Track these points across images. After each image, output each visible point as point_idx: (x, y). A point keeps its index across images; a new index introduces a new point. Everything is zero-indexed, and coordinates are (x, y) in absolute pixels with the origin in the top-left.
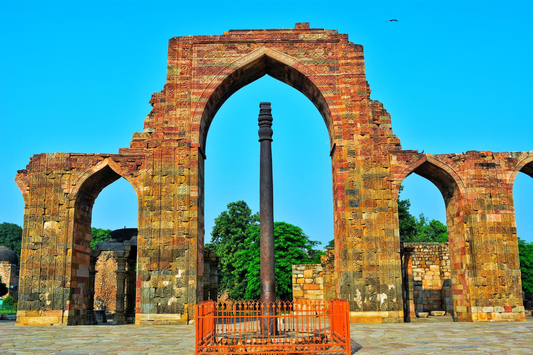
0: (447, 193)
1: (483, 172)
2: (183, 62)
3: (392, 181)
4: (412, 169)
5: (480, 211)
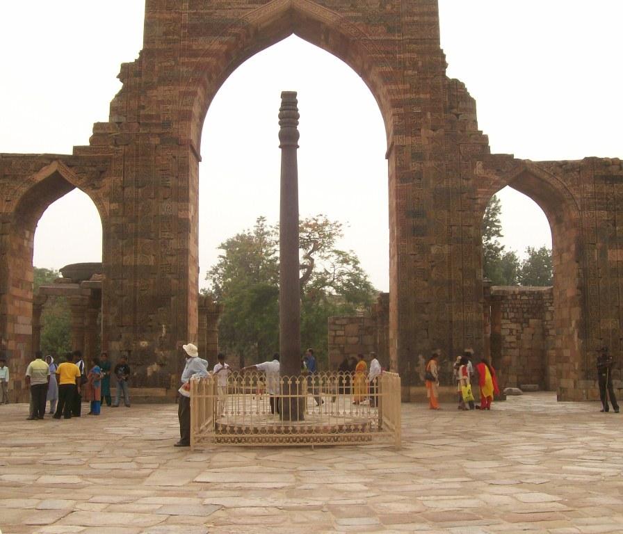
0: (554, 217)
1: (606, 189)
2: (168, 16)
3: (475, 199)
5: (599, 245)
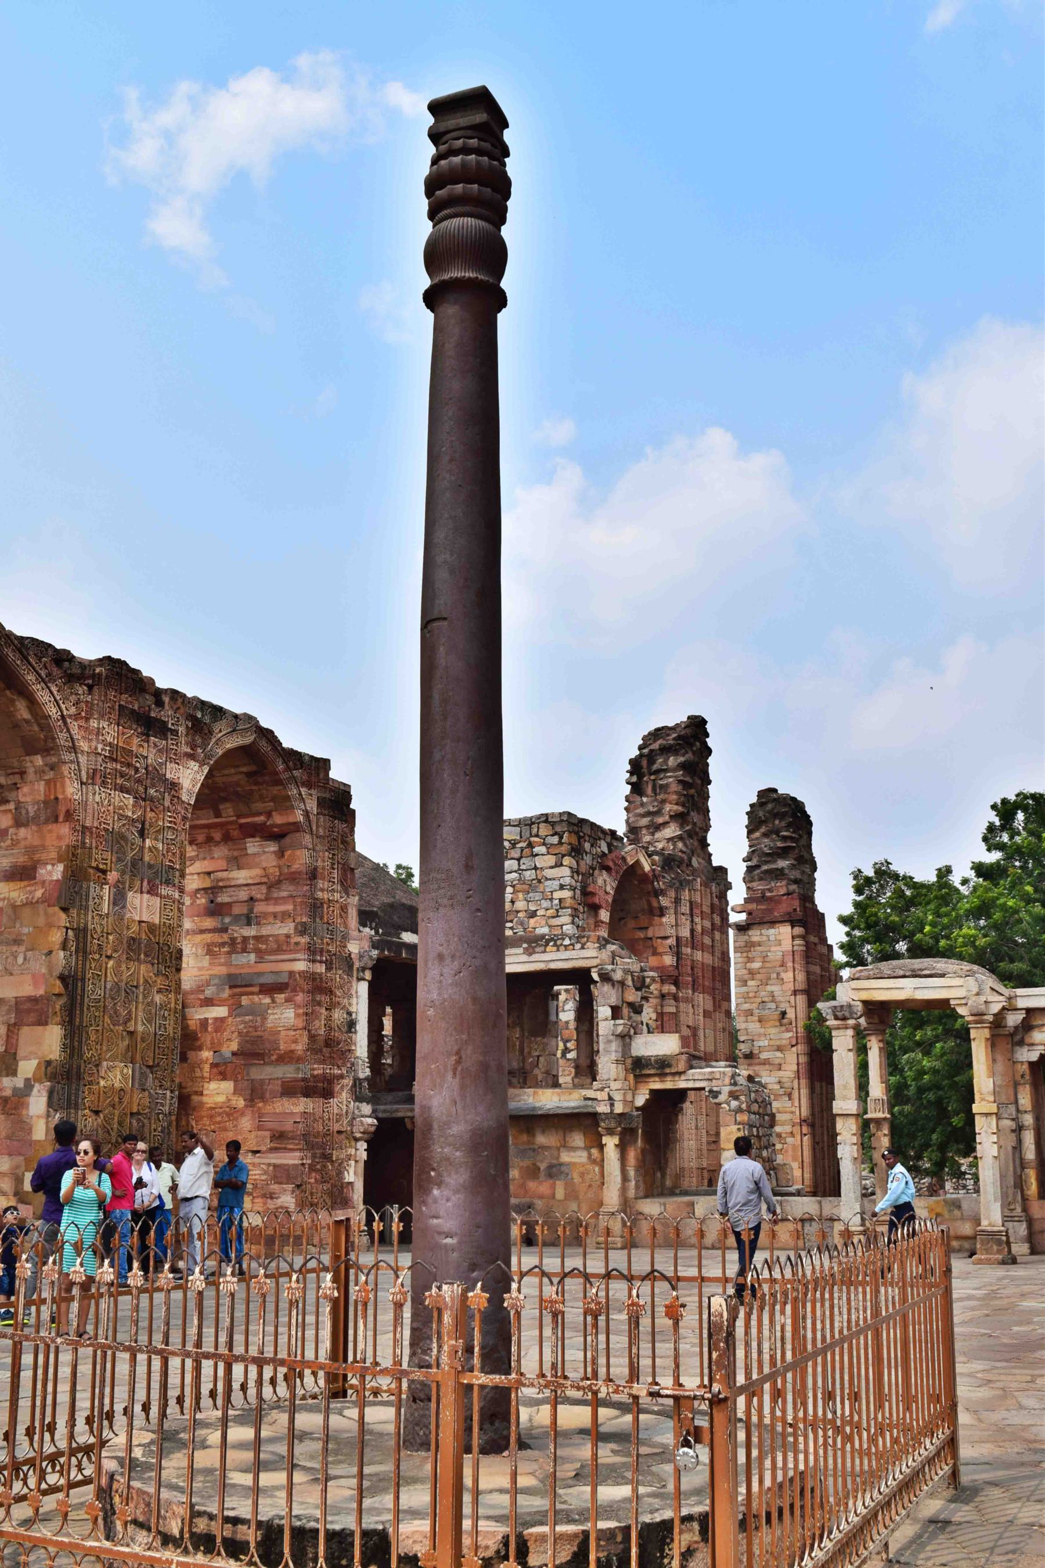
5: (113, 876)
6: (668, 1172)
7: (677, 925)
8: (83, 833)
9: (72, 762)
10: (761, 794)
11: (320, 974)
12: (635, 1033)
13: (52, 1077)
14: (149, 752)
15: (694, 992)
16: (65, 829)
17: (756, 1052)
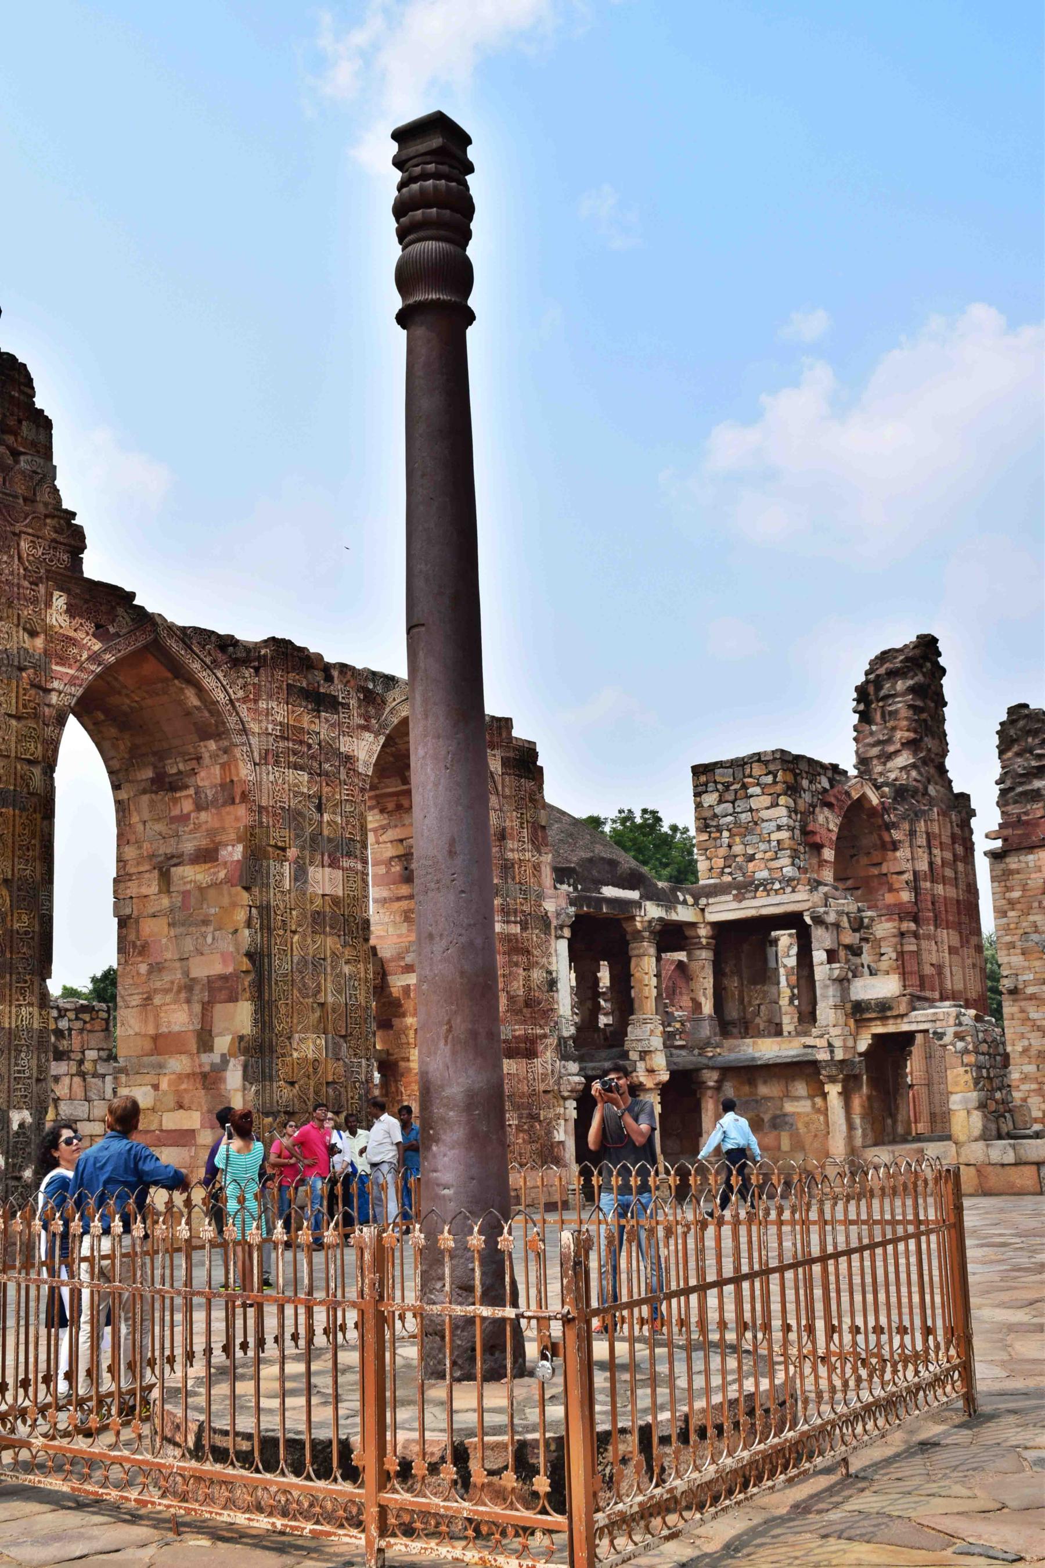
1: (306, 721)
4: (110, 658)
5: (292, 853)
6: (900, 1117)
7: (913, 859)
8: (260, 813)
9: (243, 744)
10: (1011, 711)
11: (515, 935)
12: (855, 976)
13: (245, 1051)
14: (320, 727)
15: (936, 927)
16: (241, 810)
17: (1021, 986)
